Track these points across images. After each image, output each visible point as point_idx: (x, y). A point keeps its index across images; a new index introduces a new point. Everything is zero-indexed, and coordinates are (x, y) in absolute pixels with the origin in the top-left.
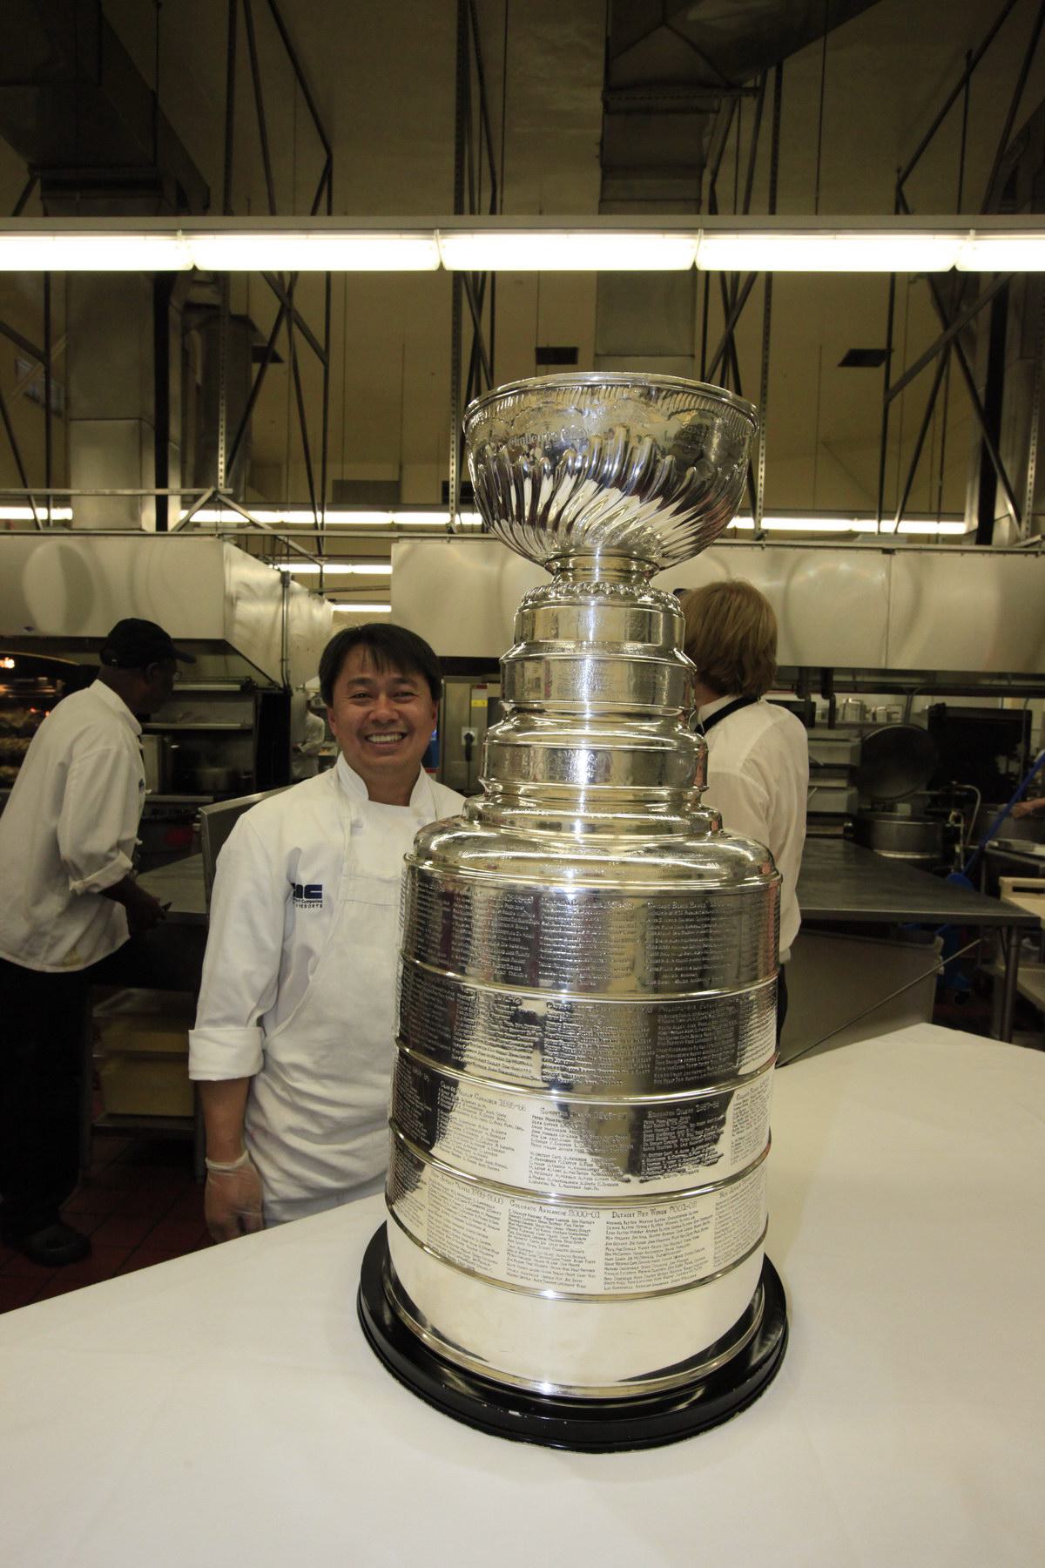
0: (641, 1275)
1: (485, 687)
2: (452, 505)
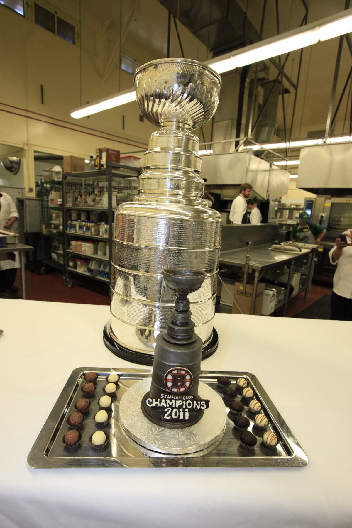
0: (134, 320)
2: (327, 133)
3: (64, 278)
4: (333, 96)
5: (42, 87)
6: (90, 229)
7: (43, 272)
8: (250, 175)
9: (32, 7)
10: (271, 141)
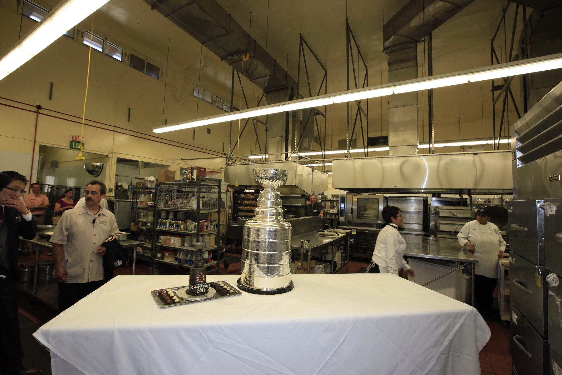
1: (356, 196)
3: (151, 268)
4: (348, 128)
5: (130, 109)
6: (180, 226)
7: (127, 264)
8: (297, 178)
9: (128, 56)
10: (311, 150)
